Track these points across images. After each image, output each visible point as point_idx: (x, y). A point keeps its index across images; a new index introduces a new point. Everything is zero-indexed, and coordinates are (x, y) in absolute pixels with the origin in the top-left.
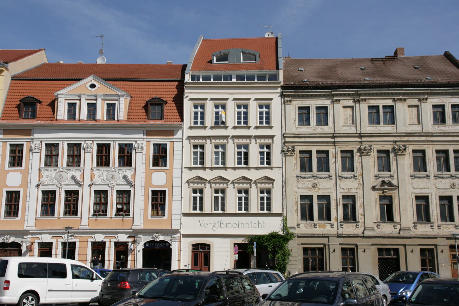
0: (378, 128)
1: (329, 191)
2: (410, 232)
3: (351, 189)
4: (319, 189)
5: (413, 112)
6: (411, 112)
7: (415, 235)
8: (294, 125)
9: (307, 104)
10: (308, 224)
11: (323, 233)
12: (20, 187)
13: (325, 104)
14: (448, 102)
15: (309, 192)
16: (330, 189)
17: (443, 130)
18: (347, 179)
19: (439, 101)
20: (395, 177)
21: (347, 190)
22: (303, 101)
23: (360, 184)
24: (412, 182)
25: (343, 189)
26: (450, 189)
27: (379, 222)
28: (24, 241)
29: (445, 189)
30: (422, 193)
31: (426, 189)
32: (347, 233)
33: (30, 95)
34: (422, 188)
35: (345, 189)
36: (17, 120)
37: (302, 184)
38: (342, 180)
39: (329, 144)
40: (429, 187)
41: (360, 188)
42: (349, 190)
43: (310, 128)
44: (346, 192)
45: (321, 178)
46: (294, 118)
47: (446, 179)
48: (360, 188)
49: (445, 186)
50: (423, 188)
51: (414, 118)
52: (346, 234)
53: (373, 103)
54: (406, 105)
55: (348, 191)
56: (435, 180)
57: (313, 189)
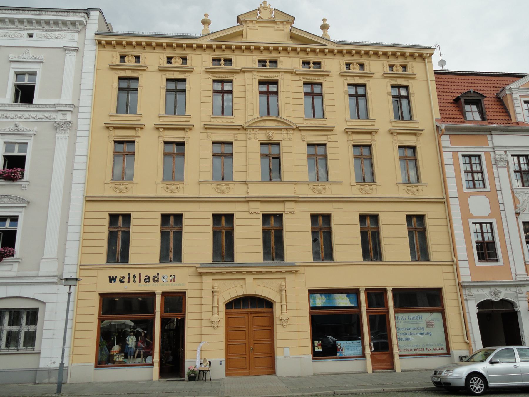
12: (489, 217)
28: (520, 298)
33: (472, 89)
36: (463, 122)
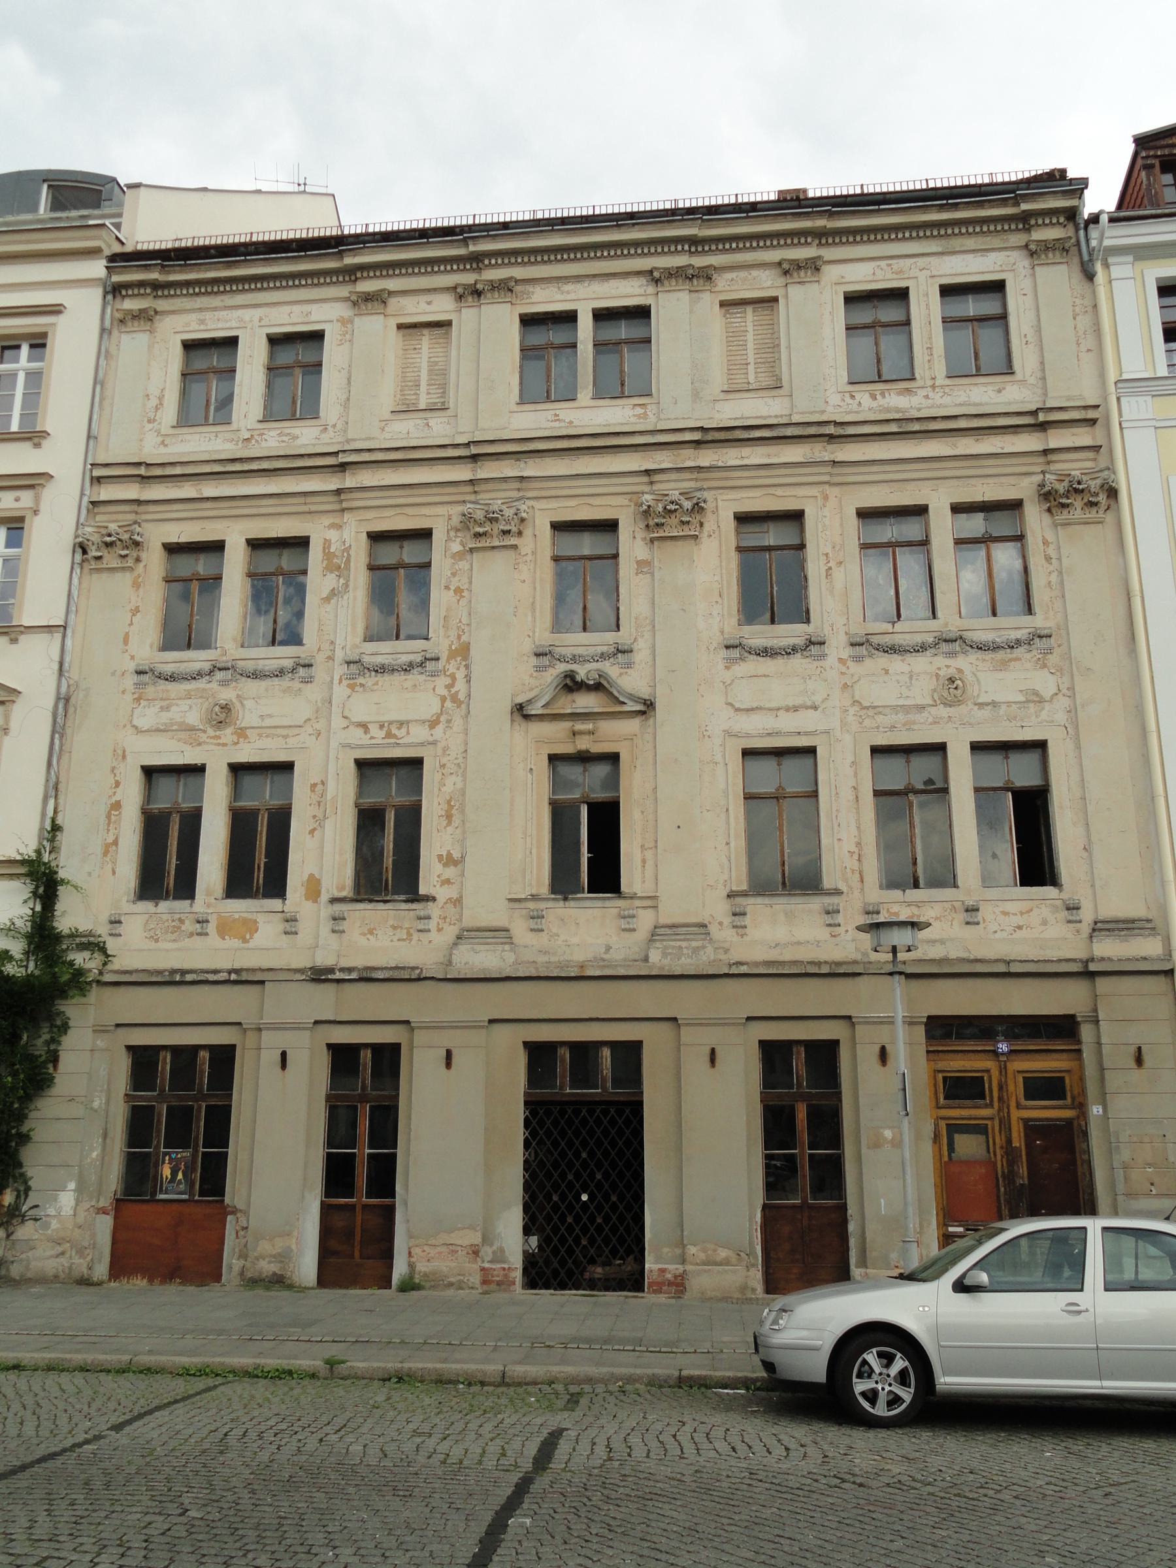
0: (563, 415)
1: (292, 742)
2: (704, 947)
3: (401, 724)
4: (242, 733)
5: (750, 337)
6: (734, 339)
7: (730, 965)
8: (151, 426)
9: (228, 325)
10: (165, 917)
11: (237, 966)
13: (313, 318)
14: (928, 273)
15: (187, 748)
16: (296, 731)
17: (898, 410)
18: (386, 677)
19: (878, 272)
20: (641, 655)
21: (383, 733)
22: (208, 315)
23: (454, 698)
24: (727, 676)
25: (364, 726)
26: (933, 710)
27: (534, 898)
29: (906, 709)
30: (778, 734)
31: (802, 714)
32: (359, 962)
34: (778, 709)
35: (374, 730)
37: (157, 709)
38: (361, 680)
39: (314, 508)
40: (818, 699)
41: (449, 721)
42: (394, 731)
43: (229, 436)
44: (373, 741)
45: (256, 675)
46: (158, 393)
47: (909, 658)
48: (449, 721)
49: (905, 692)
50: (788, 709)
51: (751, 360)
52: (350, 970)
53: (545, 300)
54: (708, 302)
55: (389, 735)
56: (850, 663)
57: (211, 732)
